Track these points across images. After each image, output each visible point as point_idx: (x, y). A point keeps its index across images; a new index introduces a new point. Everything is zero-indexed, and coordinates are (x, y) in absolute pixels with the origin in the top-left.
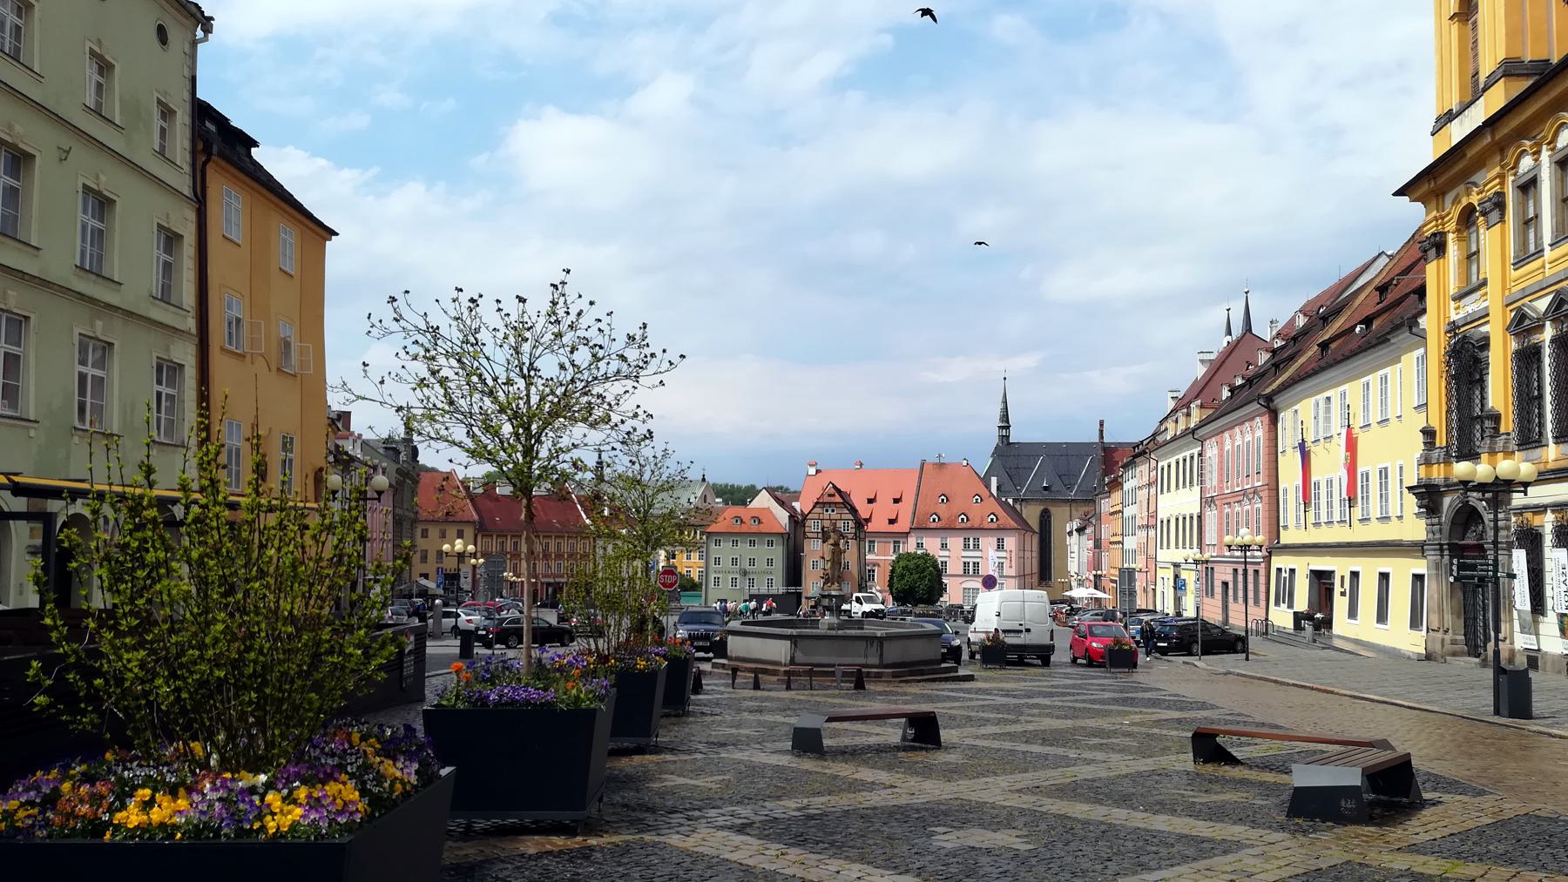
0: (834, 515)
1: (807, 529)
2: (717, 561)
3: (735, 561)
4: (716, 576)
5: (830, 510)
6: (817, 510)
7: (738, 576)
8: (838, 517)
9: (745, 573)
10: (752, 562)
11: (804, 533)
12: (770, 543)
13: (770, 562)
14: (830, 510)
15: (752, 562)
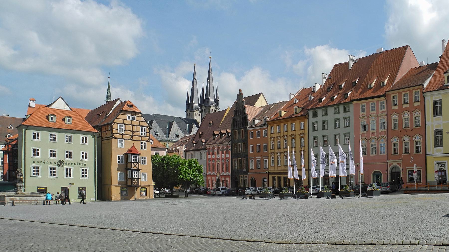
0: (134, 123)
1: (114, 131)
2: (36, 152)
3: (53, 154)
4: (36, 166)
5: (131, 117)
6: (120, 116)
7: (57, 168)
8: (137, 123)
9: (61, 163)
10: (69, 155)
11: (112, 134)
12: (85, 140)
13: (84, 155)
14: (131, 117)
15: (69, 155)
